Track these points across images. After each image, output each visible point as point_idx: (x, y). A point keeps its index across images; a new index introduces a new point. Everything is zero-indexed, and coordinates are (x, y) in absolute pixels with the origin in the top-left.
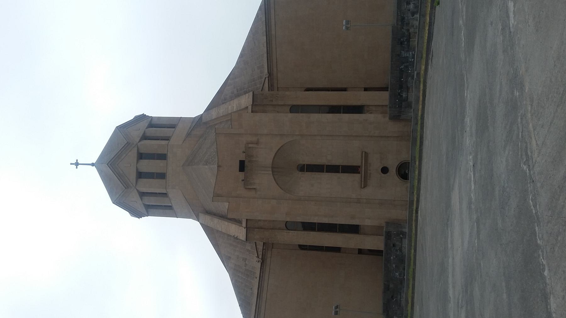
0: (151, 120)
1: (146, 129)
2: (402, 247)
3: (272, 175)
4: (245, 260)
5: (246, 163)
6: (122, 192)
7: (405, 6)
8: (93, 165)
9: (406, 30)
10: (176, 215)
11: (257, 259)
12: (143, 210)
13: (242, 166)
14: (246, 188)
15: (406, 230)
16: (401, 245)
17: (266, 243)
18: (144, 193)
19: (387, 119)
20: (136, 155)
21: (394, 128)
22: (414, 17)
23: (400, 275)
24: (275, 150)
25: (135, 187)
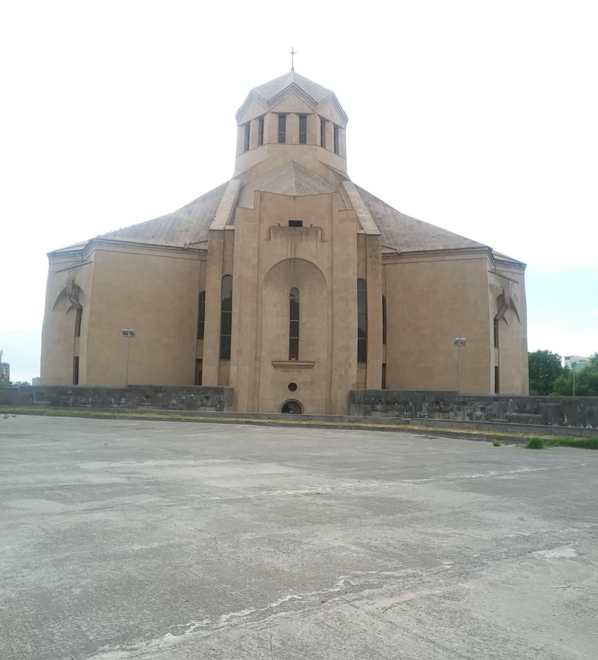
0: (343, 128)
2: (206, 406)
3: (286, 258)
4: (187, 230)
5: (299, 228)
6: (264, 99)
7: (479, 406)
9: (452, 408)
10: (238, 156)
11: (188, 243)
12: (244, 120)
14: (270, 228)
15: (225, 411)
16: (209, 406)
17: (207, 253)
18: (263, 121)
19: (351, 388)
21: (340, 395)
22: (466, 416)
23: (174, 405)
24: (314, 262)
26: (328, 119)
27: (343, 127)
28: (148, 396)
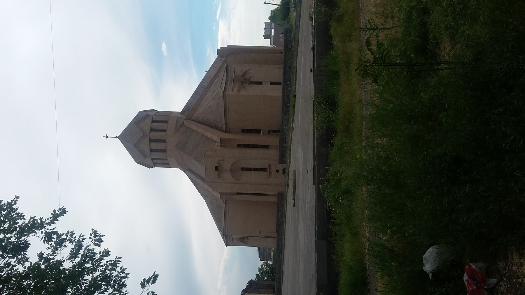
0: (152, 119)
1: (151, 124)
5: (219, 169)
8: (117, 137)
13: (217, 168)
20: (149, 140)
23: (282, 220)
25: (150, 157)
26: (150, 128)
27: (152, 117)
28: (279, 227)
